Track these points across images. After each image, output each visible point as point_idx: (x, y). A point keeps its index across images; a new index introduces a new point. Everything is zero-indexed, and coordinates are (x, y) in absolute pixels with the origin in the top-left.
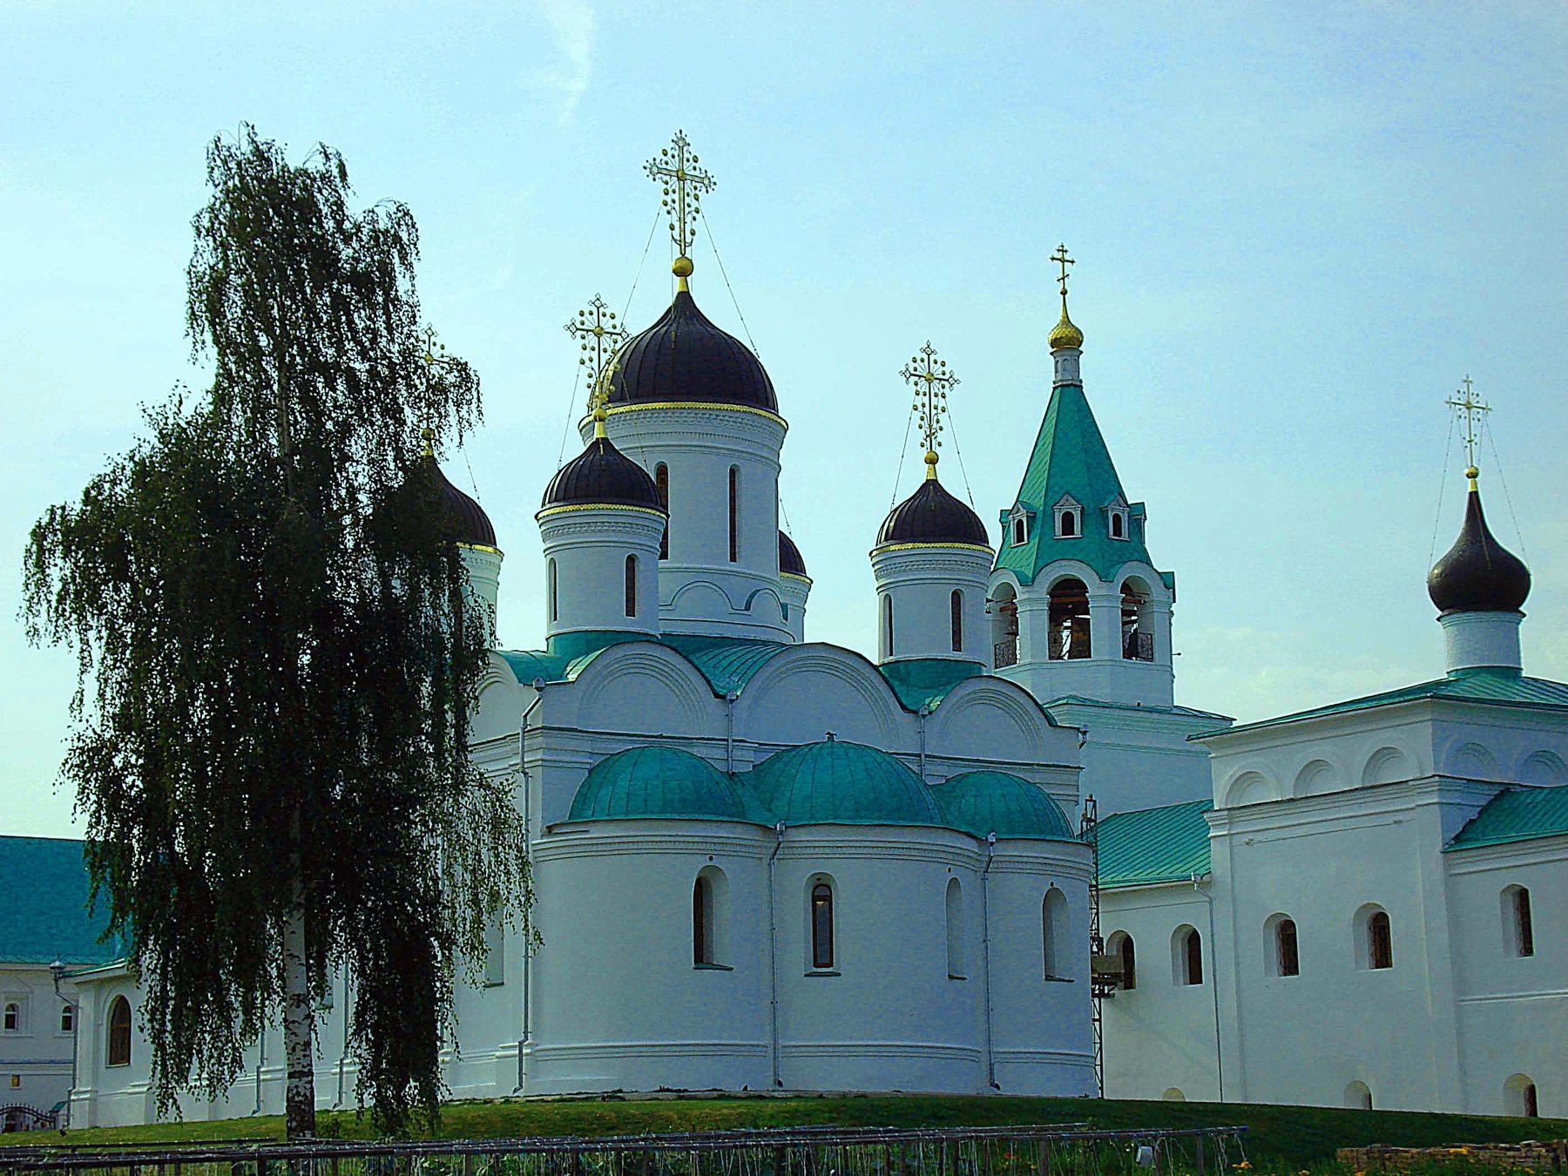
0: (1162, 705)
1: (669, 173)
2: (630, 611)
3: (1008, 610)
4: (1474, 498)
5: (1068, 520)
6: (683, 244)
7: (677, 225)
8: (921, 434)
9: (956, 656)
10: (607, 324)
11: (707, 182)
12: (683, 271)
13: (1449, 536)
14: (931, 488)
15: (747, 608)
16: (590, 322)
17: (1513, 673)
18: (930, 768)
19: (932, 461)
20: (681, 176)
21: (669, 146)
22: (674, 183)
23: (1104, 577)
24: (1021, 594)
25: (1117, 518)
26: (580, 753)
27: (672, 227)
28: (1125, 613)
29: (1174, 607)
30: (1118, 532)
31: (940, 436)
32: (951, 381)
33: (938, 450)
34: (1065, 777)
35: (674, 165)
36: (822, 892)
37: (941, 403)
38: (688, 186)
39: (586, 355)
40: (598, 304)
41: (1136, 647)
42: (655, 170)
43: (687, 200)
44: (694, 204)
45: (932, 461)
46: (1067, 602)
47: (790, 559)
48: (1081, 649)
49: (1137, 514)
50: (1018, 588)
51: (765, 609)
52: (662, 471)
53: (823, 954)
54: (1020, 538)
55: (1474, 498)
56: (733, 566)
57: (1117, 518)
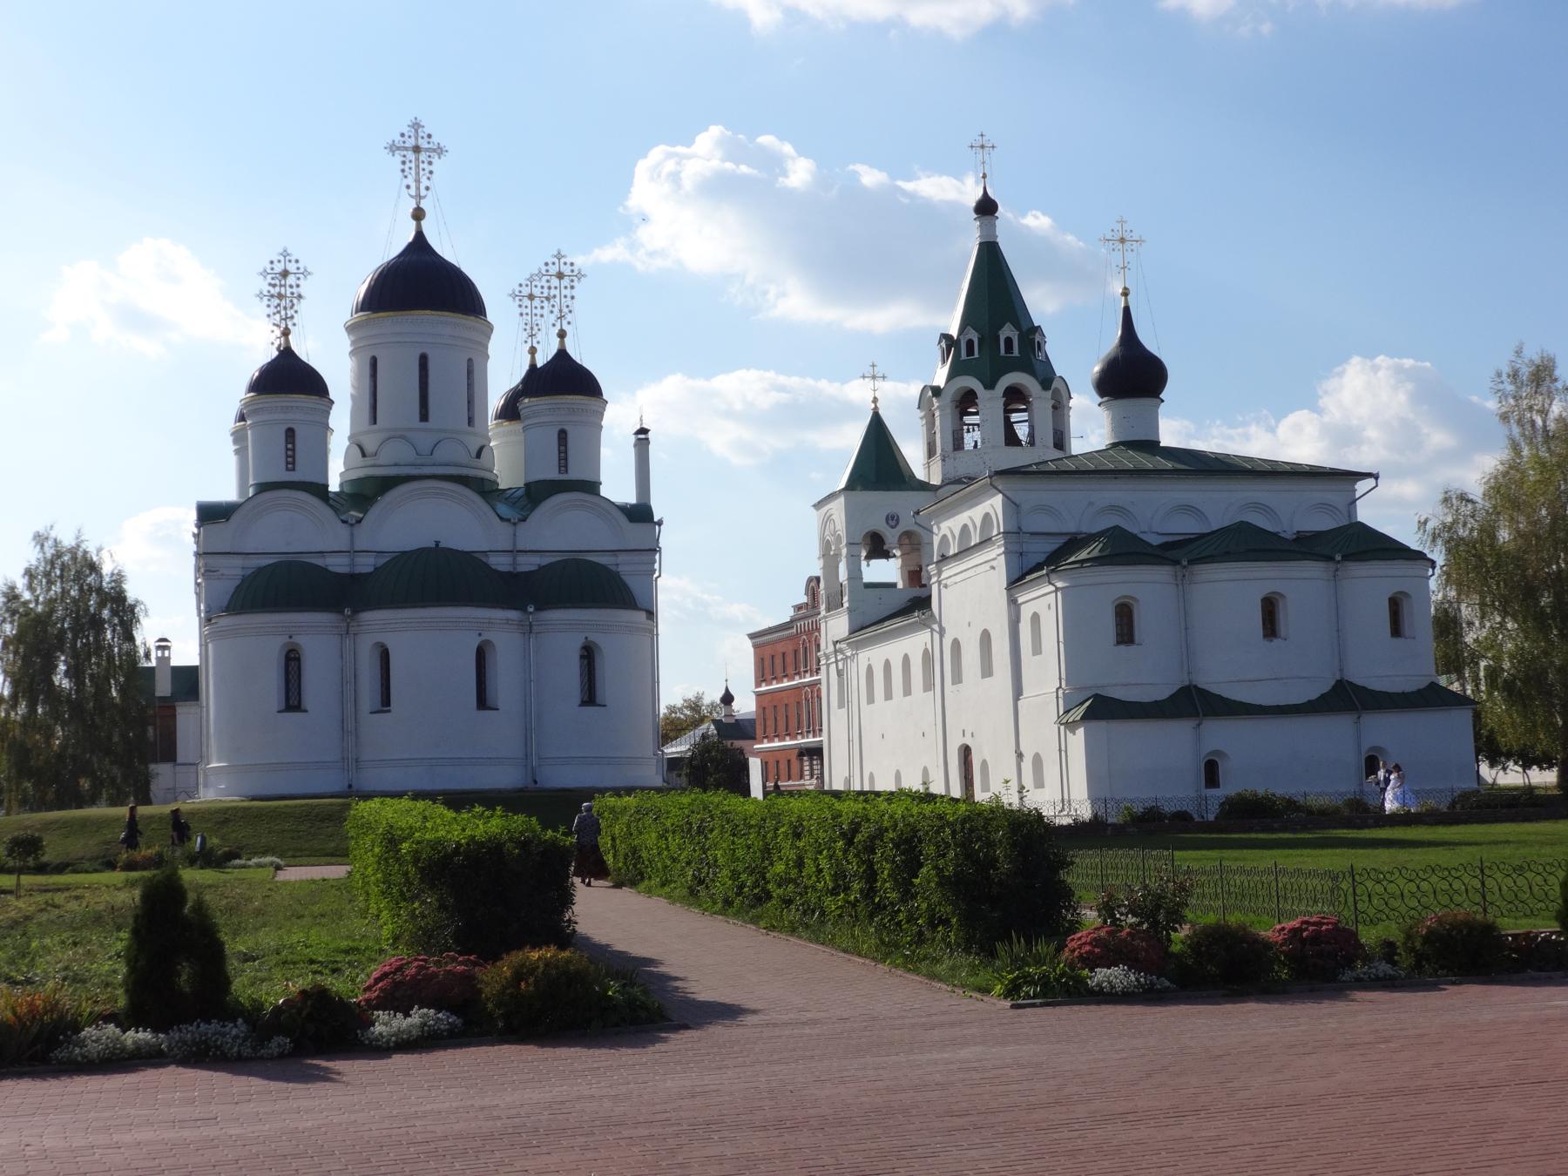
1: (406, 149)
2: (291, 463)
4: (1127, 311)
5: (970, 343)
6: (419, 197)
7: (413, 185)
8: (552, 318)
10: (292, 267)
11: (440, 151)
12: (418, 215)
13: (1111, 339)
14: (562, 354)
17: (1150, 446)
18: (521, 559)
20: (417, 149)
21: (406, 130)
22: (411, 155)
23: (990, 385)
25: (1009, 341)
26: (235, 570)
31: (569, 317)
33: (565, 327)
34: (644, 557)
35: (411, 143)
36: (385, 656)
38: (423, 156)
40: (285, 254)
42: (393, 148)
45: (562, 335)
49: (1031, 336)
54: (944, 362)
55: (1127, 311)
57: (1009, 341)
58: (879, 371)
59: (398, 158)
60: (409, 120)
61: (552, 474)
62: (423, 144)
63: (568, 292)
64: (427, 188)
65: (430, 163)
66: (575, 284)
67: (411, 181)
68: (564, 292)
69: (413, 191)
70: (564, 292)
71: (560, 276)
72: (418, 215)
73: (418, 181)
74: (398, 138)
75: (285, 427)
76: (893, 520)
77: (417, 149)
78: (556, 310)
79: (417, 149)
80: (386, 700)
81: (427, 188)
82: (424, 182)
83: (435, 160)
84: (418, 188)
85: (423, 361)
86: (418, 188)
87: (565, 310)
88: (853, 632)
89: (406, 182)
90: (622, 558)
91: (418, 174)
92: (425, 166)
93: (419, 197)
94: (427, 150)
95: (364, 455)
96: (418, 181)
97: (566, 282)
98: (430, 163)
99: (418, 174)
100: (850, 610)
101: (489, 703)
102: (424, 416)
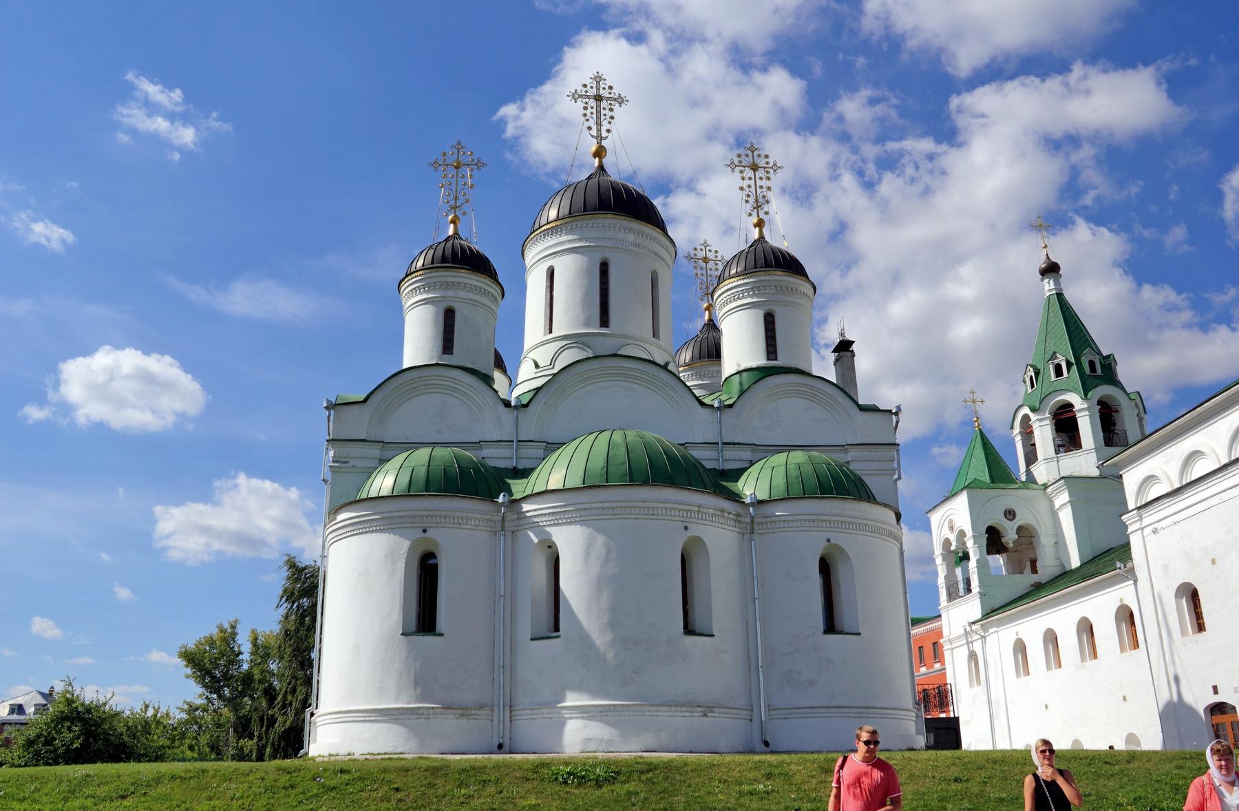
1: (588, 97)
6: (599, 138)
7: (594, 128)
8: (749, 207)
9: (772, 363)
22: (592, 103)
25: (1092, 364)
27: (589, 128)
33: (762, 216)
35: (593, 92)
37: (764, 183)
38: (604, 104)
40: (459, 147)
43: (603, 112)
50: (1031, 414)
56: (604, 330)
58: (978, 397)
59: (580, 104)
60: (591, 73)
62: (605, 93)
63: (764, 183)
64: (608, 131)
65: (611, 110)
66: (771, 175)
67: (592, 123)
69: (594, 132)
72: (600, 153)
73: (599, 124)
75: (444, 305)
76: (1010, 514)
77: (598, 98)
78: (751, 200)
79: (598, 98)
81: (608, 131)
82: (605, 126)
83: (616, 107)
84: (599, 130)
85: (604, 268)
86: (599, 130)
87: (761, 200)
88: (987, 615)
89: (588, 124)
90: (851, 455)
91: (599, 118)
92: (607, 112)
93: (599, 138)
94: (608, 99)
95: (537, 366)
96: (599, 124)
98: (611, 110)
99: (599, 118)
100: (982, 595)
101: (698, 625)
102: (605, 322)
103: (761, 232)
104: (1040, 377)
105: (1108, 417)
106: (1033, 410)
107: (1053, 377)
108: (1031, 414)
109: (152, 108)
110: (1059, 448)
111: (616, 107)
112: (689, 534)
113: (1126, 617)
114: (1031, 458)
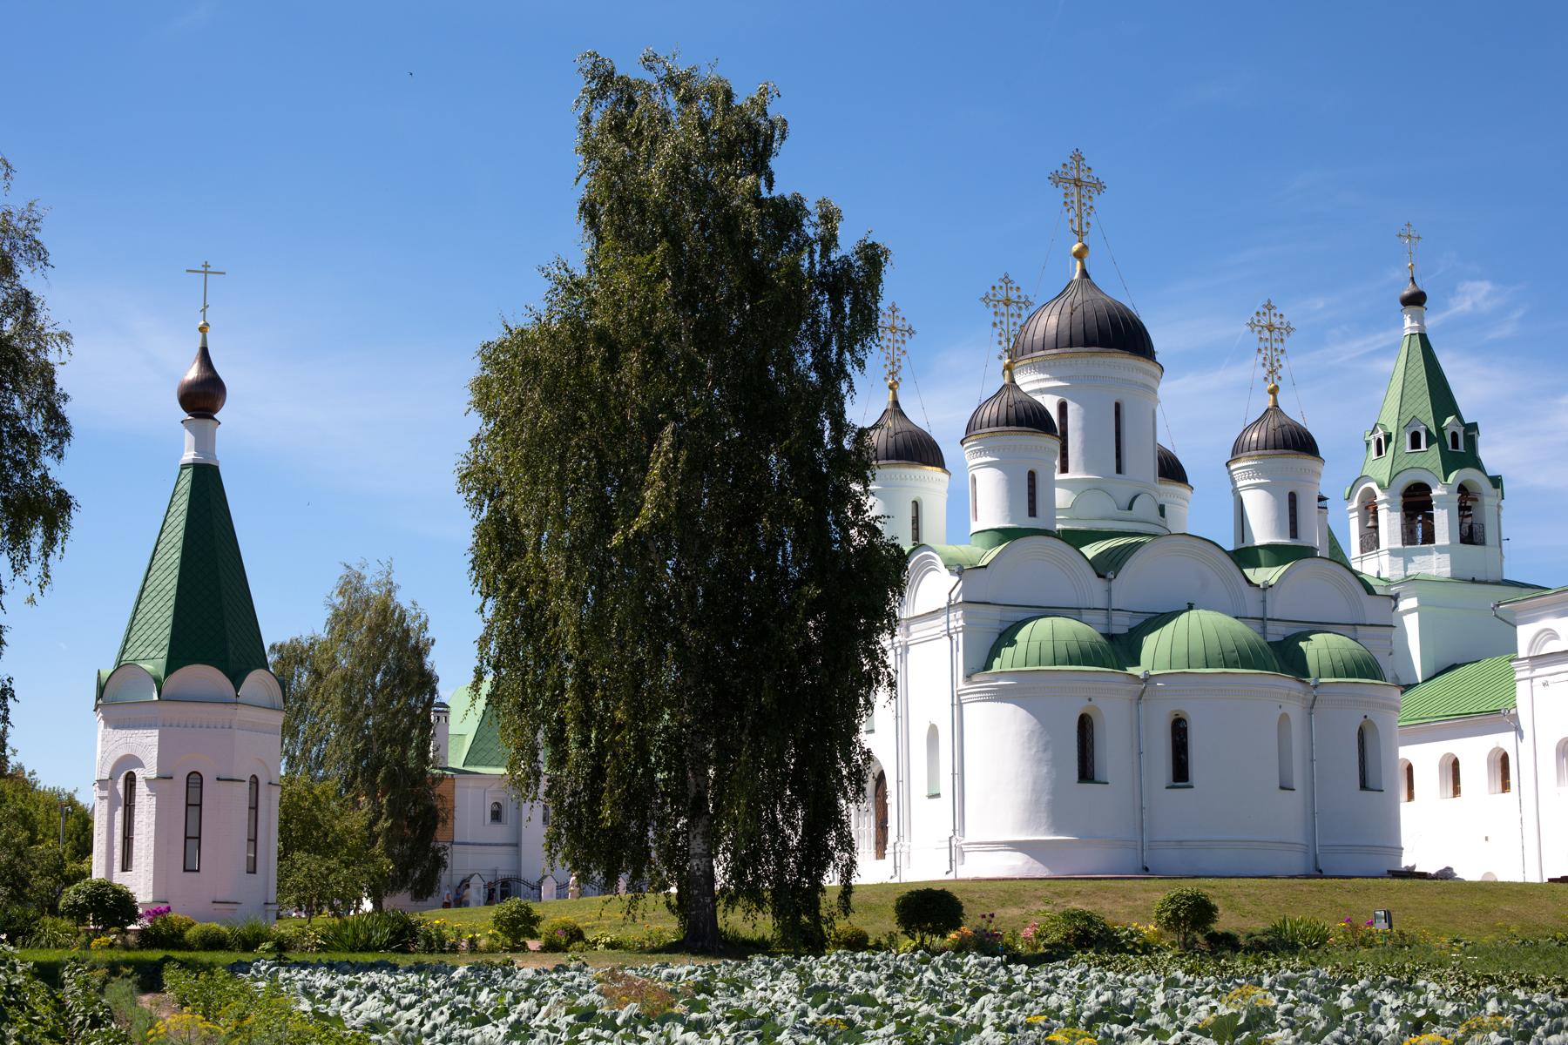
0: (1492, 577)
1: (1067, 181)
2: (1032, 512)
3: (1369, 510)
7: (1076, 221)
8: (1264, 372)
10: (1013, 295)
11: (1099, 186)
15: (1130, 508)
16: (1001, 295)
19: (1274, 392)
20: (1078, 182)
24: (1380, 496)
25: (1454, 435)
28: (1461, 508)
29: (1503, 503)
30: (1455, 445)
32: (1289, 330)
36: (1179, 730)
37: (1280, 347)
39: (997, 320)
40: (1006, 280)
41: (1470, 535)
42: (1057, 179)
44: (1089, 204)
46: (1416, 503)
47: (1171, 470)
48: (1429, 537)
50: (1378, 492)
51: (1144, 508)
52: (1063, 408)
53: (1181, 773)
54: (1379, 452)
57: (1454, 435)
61: (1286, 541)
68: (1275, 345)
70: (1275, 345)
71: (1270, 328)
74: (1061, 169)
80: (1181, 773)
83: (1095, 195)
97: (1276, 334)
103: (1275, 400)
104: (1392, 445)
105: (1466, 499)
106: (1381, 486)
107: (1408, 449)
108: (1378, 492)
109: (812, 263)
110: (1409, 537)
111: (1095, 195)
112: (1283, 710)
113: (1503, 764)
114: (1370, 541)
